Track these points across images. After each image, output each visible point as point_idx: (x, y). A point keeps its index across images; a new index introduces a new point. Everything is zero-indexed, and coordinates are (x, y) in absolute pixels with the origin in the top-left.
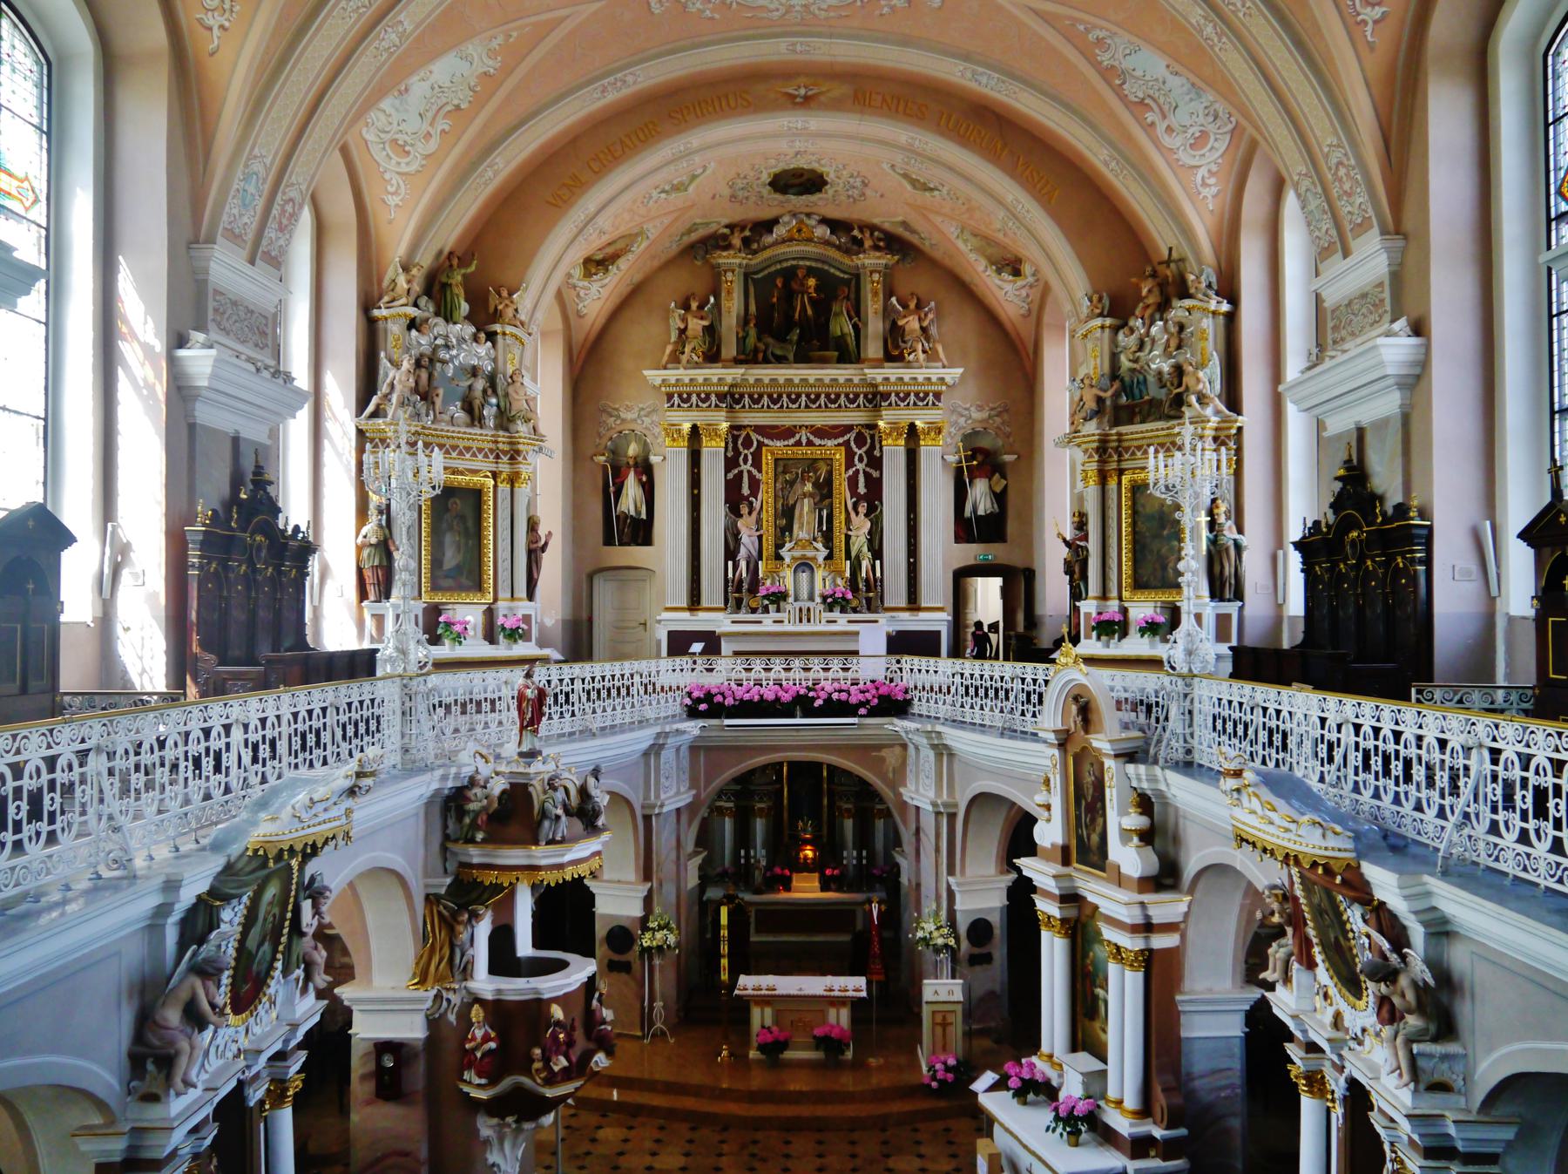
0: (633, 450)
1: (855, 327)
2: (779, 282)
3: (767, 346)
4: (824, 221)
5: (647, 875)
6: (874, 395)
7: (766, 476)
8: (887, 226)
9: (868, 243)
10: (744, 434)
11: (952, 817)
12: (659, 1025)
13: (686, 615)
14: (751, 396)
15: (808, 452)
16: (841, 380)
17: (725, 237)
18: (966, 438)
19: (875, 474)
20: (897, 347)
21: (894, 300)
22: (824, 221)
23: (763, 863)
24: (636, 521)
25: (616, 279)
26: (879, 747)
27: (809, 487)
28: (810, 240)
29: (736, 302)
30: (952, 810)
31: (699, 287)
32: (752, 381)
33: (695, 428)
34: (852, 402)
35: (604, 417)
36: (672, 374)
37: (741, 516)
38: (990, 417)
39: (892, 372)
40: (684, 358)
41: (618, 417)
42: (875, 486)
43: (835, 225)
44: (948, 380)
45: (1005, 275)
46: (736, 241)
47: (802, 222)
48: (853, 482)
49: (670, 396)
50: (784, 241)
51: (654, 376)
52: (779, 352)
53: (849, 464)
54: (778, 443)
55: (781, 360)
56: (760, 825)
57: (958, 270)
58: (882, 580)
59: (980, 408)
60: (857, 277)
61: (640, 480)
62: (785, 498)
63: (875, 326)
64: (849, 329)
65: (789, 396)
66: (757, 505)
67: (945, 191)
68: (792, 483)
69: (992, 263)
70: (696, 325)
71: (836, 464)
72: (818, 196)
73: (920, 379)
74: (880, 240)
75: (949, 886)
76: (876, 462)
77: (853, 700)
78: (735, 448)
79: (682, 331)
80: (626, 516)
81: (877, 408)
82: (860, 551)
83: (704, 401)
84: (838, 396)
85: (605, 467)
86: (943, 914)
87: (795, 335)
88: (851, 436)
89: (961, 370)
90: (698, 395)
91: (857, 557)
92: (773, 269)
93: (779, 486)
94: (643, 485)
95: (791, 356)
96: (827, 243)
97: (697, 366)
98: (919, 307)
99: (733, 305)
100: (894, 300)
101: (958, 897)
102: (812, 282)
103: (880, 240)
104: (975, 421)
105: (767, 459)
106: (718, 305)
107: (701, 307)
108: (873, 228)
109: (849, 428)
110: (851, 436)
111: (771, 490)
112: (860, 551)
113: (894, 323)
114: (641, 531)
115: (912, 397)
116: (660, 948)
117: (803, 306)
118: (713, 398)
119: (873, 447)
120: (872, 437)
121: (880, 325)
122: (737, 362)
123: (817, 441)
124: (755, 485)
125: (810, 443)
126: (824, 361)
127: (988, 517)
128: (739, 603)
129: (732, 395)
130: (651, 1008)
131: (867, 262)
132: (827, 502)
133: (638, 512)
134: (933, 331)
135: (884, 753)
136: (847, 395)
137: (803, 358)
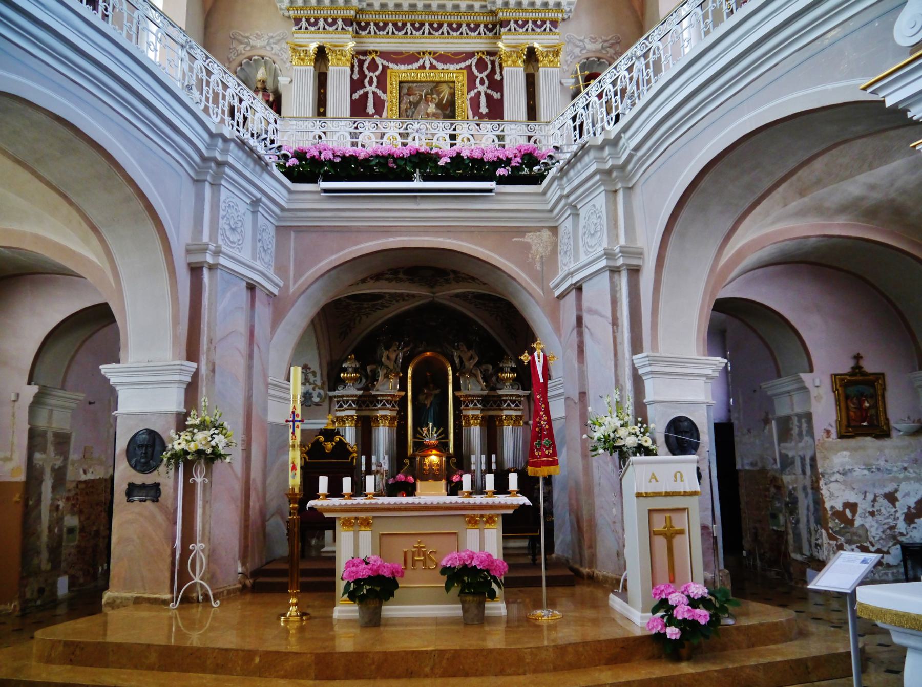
5: (192, 354)
10: (369, 58)
11: (634, 272)
12: (197, 579)
14: (376, 24)
15: (432, 76)
18: (583, 67)
19: (496, 96)
23: (385, 467)
26: (521, 231)
27: (432, 108)
30: (635, 262)
34: (474, 30)
35: (235, 44)
38: (603, 48)
41: (248, 44)
49: (297, 21)
53: (471, 85)
54: (403, 67)
56: (383, 435)
59: (594, 40)
61: (267, 101)
65: (413, 25)
68: (416, 105)
71: (458, 86)
75: (635, 370)
76: (497, 86)
78: (361, 71)
81: (497, 36)
83: (331, 25)
84: (460, 25)
86: (629, 405)
88: (473, 61)
90: (326, 20)
101: (650, 386)
104: (589, 51)
109: (471, 55)
110: (473, 61)
111: (396, 109)
115: (530, 24)
116: (200, 453)
118: (340, 22)
119: (493, 71)
120: (493, 63)
123: (440, 66)
125: (433, 67)
129: (359, 24)
130: (186, 552)
135: (529, 238)
136: (468, 25)
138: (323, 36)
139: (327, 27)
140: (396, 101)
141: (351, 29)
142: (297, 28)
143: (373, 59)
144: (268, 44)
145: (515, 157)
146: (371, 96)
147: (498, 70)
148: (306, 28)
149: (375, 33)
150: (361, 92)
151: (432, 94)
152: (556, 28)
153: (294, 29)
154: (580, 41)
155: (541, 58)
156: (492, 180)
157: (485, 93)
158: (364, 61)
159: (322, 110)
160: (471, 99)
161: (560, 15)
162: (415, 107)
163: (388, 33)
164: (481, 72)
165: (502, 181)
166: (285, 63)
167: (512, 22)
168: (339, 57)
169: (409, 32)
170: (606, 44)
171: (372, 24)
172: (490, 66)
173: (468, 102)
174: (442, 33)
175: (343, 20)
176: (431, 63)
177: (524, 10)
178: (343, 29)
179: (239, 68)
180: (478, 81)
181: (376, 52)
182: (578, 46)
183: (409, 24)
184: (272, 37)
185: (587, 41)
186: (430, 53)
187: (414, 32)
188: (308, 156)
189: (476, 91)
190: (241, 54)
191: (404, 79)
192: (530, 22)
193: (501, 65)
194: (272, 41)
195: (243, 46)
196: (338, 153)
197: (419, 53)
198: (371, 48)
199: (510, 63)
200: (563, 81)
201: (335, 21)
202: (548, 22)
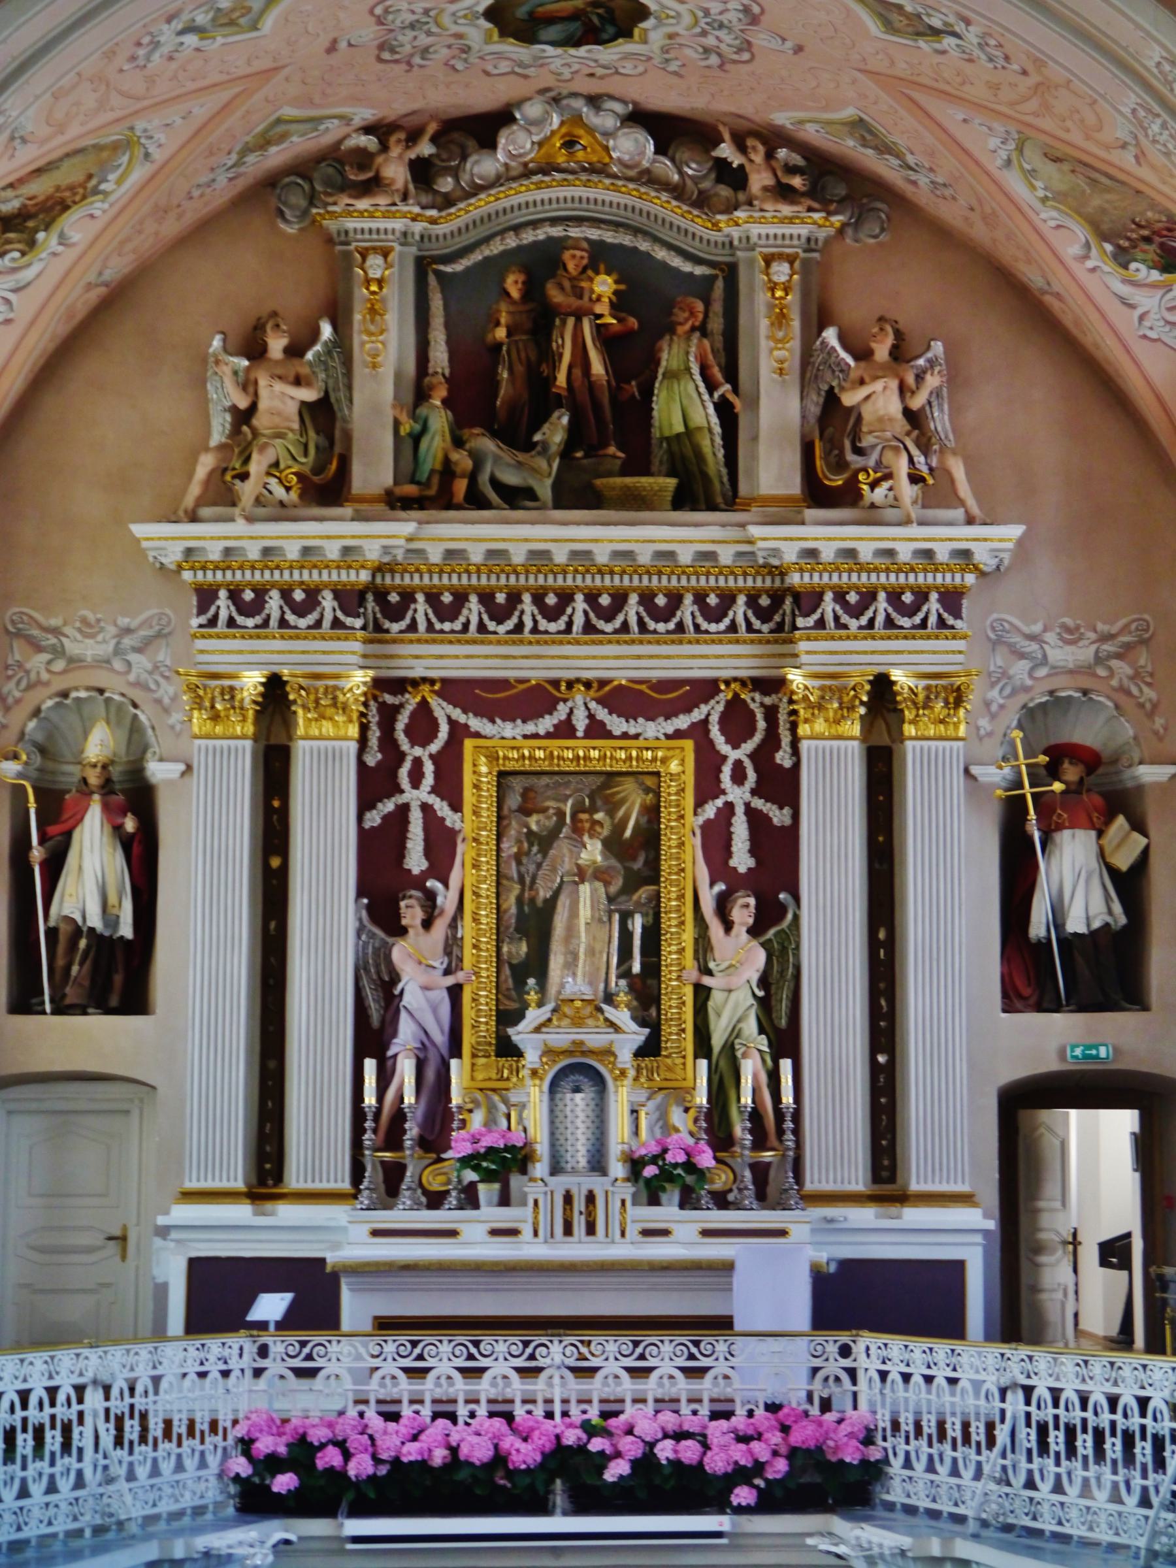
0: (99, 744)
1: (725, 410)
2: (513, 284)
3: (478, 460)
4: (639, 117)
6: (777, 597)
7: (474, 820)
8: (812, 134)
9: (759, 180)
10: (412, 701)
13: (242, 1212)
14: (433, 598)
15: (594, 753)
16: (685, 556)
17: (363, 159)
19: (779, 816)
20: (840, 465)
21: (830, 335)
22: (639, 117)
24: (104, 946)
25: (58, 268)
27: (593, 852)
28: (598, 170)
29: (392, 337)
31: (293, 290)
32: (435, 555)
33: (275, 686)
35: (18, 651)
36: (213, 536)
37: (402, 932)
38: (1099, 660)
39: (827, 534)
40: (247, 491)
41: (58, 652)
42: (778, 852)
43: (668, 129)
44: (983, 556)
45: (1140, 270)
46: (396, 171)
47: (578, 119)
48: (716, 839)
49: (206, 596)
50: (527, 173)
51: (164, 539)
52: (511, 478)
53: (707, 787)
54: (510, 730)
55: (516, 498)
57: (1007, 254)
58: (797, 1116)
59: (1071, 636)
60: (730, 272)
61: (118, 829)
62: (527, 883)
63: (778, 412)
64: (705, 415)
65: (538, 599)
66: (447, 900)
67: (972, 35)
68: (545, 841)
69: (1104, 237)
70: (281, 401)
71: (669, 790)
72: (622, 47)
73: (905, 553)
74: (791, 170)
76: (781, 785)
77: (717, 1463)
79: (243, 417)
80: (77, 932)
81: (784, 632)
82: (735, 1033)
83: (301, 610)
84: (676, 600)
85: (18, 792)
87: (555, 431)
88: (713, 710)
89: (1015, 531)
90: (286, 594)
91: (729, 1048)
92: (496, 248)
93: (510, 847)
94: (127, 843)
95: (545, 490)
96: (648, 178)
97: (282, 512)
98: (899, 354)
99: (386, 348)
100: (830, 335)
102: (604, 285)
103: (791, 170)
104: (1056, 671)
105: (477, 772)
106: (342, 345)
107: (295, 351)
108: (773, 138)
109: (706, 689)
110: (713, 710)
111: (488, 861)
112: (735, 1033)
113: (831, 399)
114: (118, 974)
115: (882, 603)
117: (580, 353)
118: (328, 602)
119: (771, 741)
120: (771, 714)
121: (794, 405)
122: (396, 502)
123: (617, 725)
124: (442, 845)
125: (597, 730)
126: (635, 502)
127: (1097, 938)
128: (393, 1177)
131: (755, 230)
132: (643, 893)
133: (111, 920)
134: (940, 421)
136: (700, 598)
137: (577, 494)
138: (278, 644)
139: (291, 618)
140: (488, 835)
141: (358, 623)
142: (203, 620)
143: (424, 703)
144: (117, 651)
145: (775, 1453)
146: (416, 819)
147: (786, 739)
148: (231, 623)
149: (430, 627)
150: (388, 806)
151: (593, 809)
152: (958, 615)
153: (195, 622)
154: (1032, 638)
155: (909, 715)
156: (722, 1512)
157: (750, 811)
158: (397, 709)
159: (275, 862)
160: (707, 827)
161: (970, 579)
162: (544, 851)
163: (466, 627)
164: (736, 746)
165: (740, 1510)
166: (167, 711)
167: (829, 596)
168: (330, 711)
169: (528, 624)
170: (1108, 647)
171: (420, 598)
172: (761, 724)
173: (698, 841)
174: (625, 628)
175: (338, 595)
176: (591, 716)
177: (862, 568)
178: (337, 624)
179: (32, 724)
180: (727, 770)
181: (432, 682)
182: (1022, 656)
183: (527, 598)
184: (128, 631)
185: (1051, 637)
186: (588, 684)
187: (543, 624)
188: (320, 1464)
189: (719, 802)
190: (39, 683)
191: (510, 766)
192: (882, 596)
193: (794, 727)
194: (127, 642)
195: (45, 657)
196: (384, 1456)
197: (555, 683)
198: (418, 672)
199: (820, 726)
200: (974, 770)
201: (313, 595)
202: (934, 596)
